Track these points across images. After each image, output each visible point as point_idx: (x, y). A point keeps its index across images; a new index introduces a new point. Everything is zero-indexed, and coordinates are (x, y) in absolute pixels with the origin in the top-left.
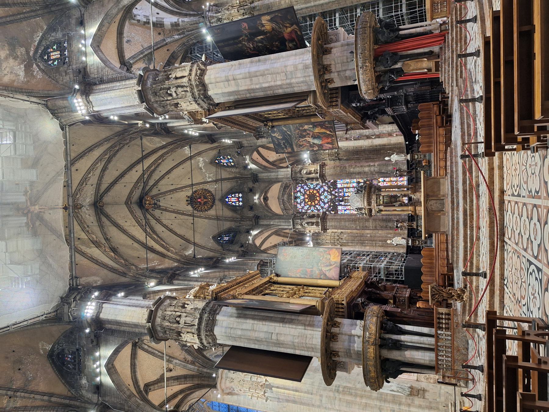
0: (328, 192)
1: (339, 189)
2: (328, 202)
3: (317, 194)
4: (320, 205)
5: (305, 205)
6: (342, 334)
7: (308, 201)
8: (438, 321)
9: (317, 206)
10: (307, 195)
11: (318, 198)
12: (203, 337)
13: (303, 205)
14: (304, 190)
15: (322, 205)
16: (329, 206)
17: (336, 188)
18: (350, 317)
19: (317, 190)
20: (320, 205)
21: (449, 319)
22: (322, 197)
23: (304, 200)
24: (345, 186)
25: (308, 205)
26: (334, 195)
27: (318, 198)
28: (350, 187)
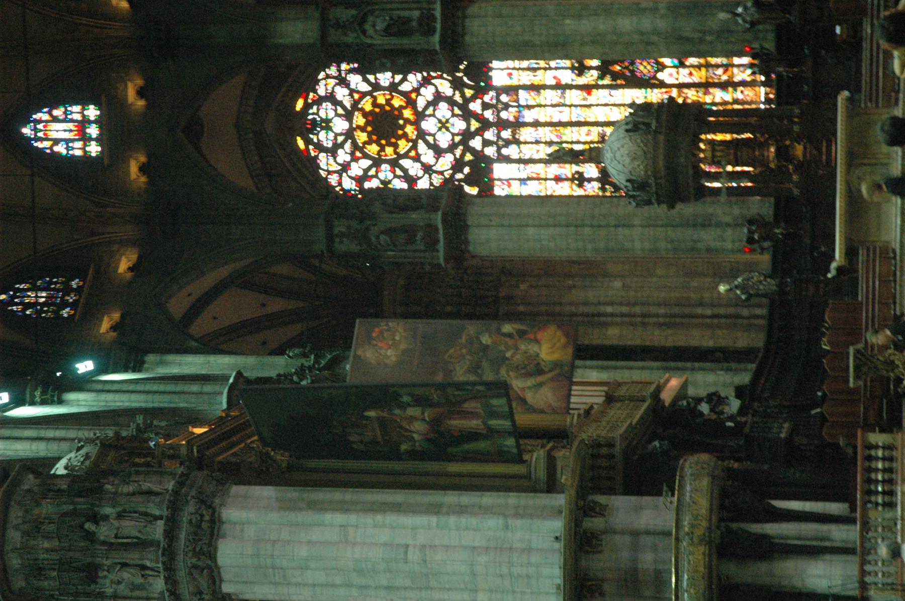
0: (451, 101)
1: (500, 90)
2: (452, 148)
3: (408, 113)
4: (417, 159)
5: (355, 159)
6: (614, 532)
7: (369, 142)
8: (866, 487)
9: (405, 163)
10: (365, 114)
11: (409, 129)
12: (182, 574)
13: (343, 156)
14: (352, 92)
15: (428, 156)
16: (458, 166)
17: (489, 87)
18: (627, 492)
19: (406, 95)
20: (417, 159)
21: (891, 459)
22: (429, 125)
23: (349, 134)
24: (526, 78)
25: (366, 156)
26: (479, 118)
27: (409, 129)
28: (545, 87)
